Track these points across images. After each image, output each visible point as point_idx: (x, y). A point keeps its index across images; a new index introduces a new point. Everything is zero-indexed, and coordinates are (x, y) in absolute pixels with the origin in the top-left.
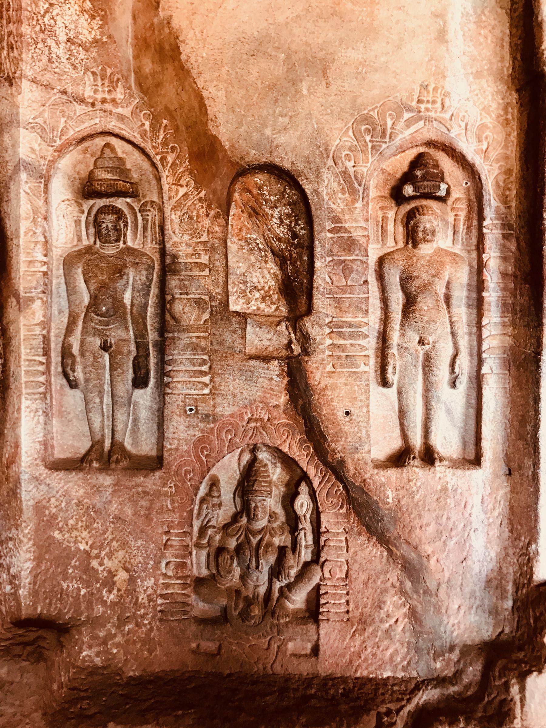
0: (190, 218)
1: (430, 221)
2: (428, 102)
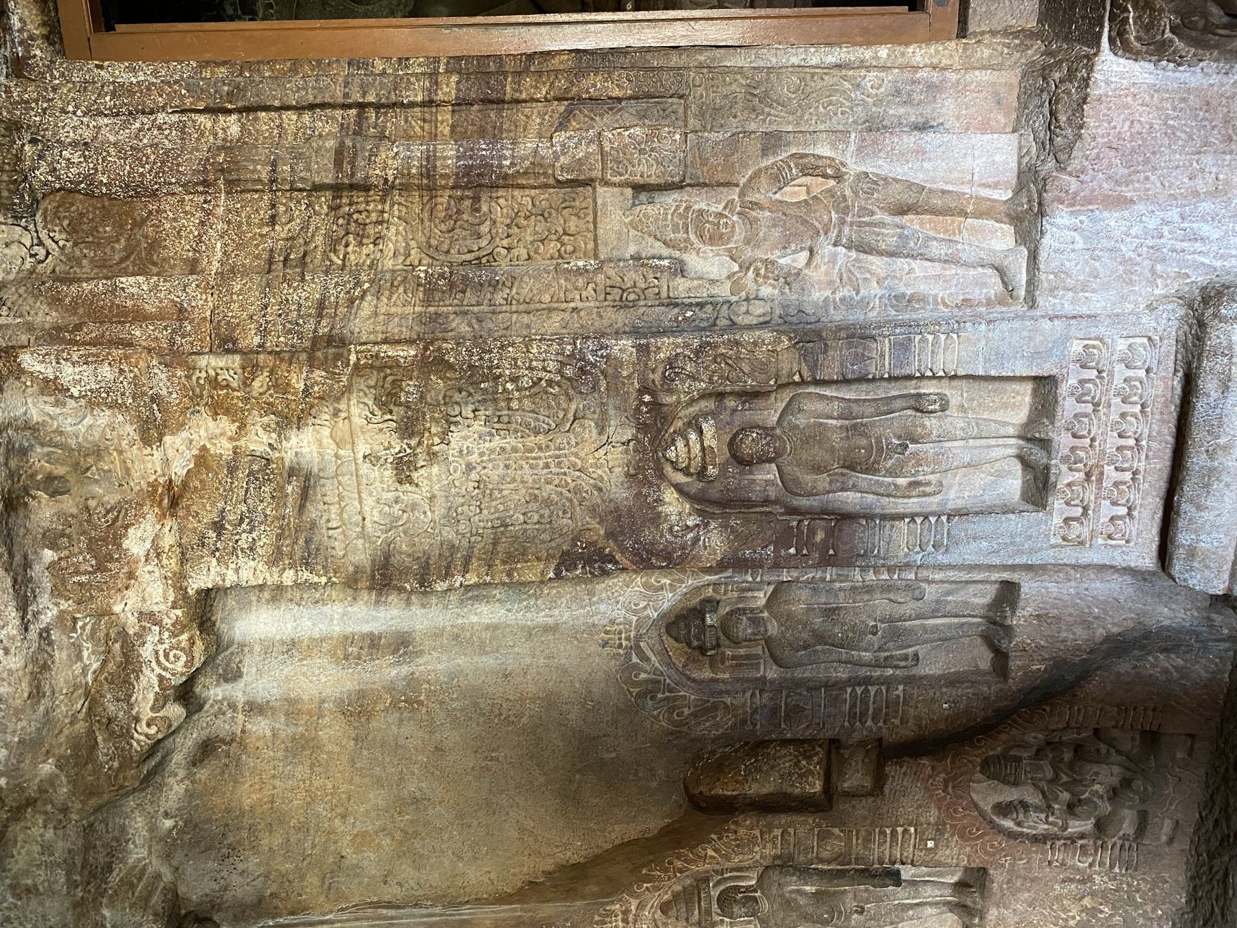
0: (738, 846)
1: (745, 630)
2: (620, 639)
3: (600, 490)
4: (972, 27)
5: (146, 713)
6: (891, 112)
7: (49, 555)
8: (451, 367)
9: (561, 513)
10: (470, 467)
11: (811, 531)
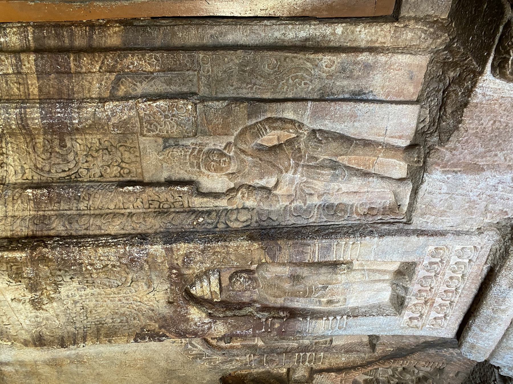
3: (153, 310)
4: (404, 13)
6: (338, 84)
8: (51, 260)
9: (132, 319)
10: (75, 302)
11: (273, 324)
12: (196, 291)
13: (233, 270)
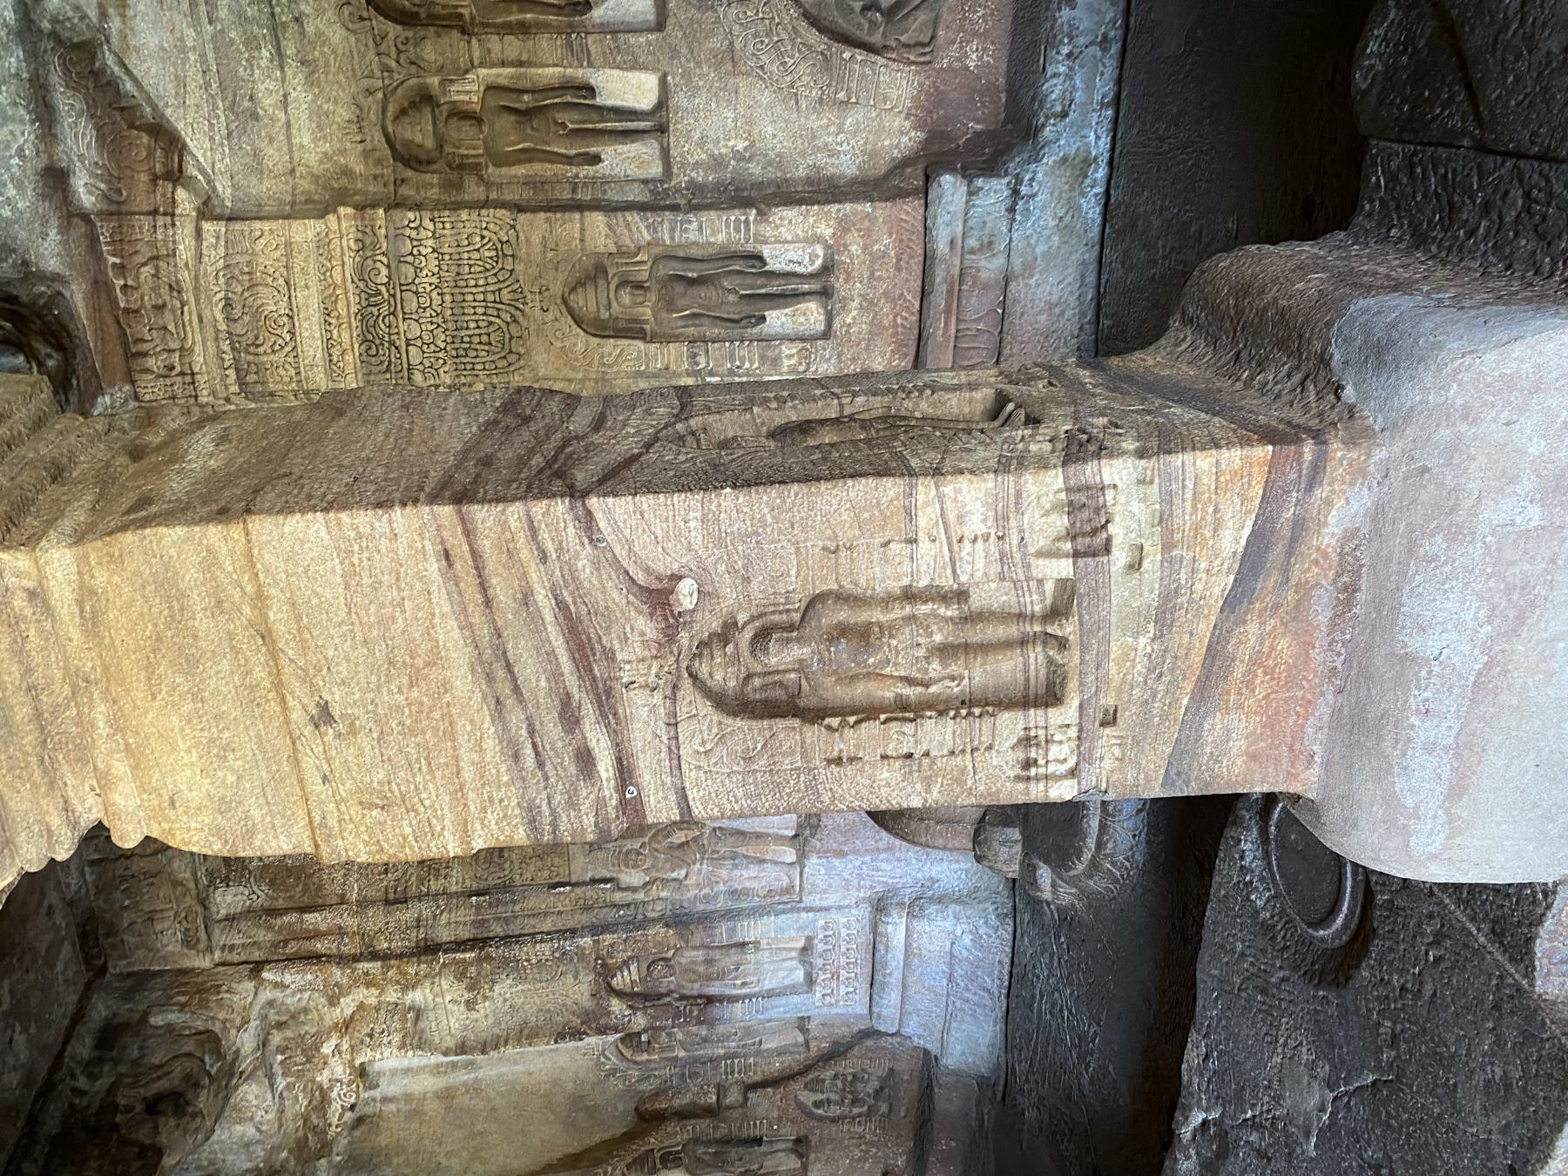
5: (335, 1121)
7: (280, 1058)
12: (617, 982)
13: (651, 958)
